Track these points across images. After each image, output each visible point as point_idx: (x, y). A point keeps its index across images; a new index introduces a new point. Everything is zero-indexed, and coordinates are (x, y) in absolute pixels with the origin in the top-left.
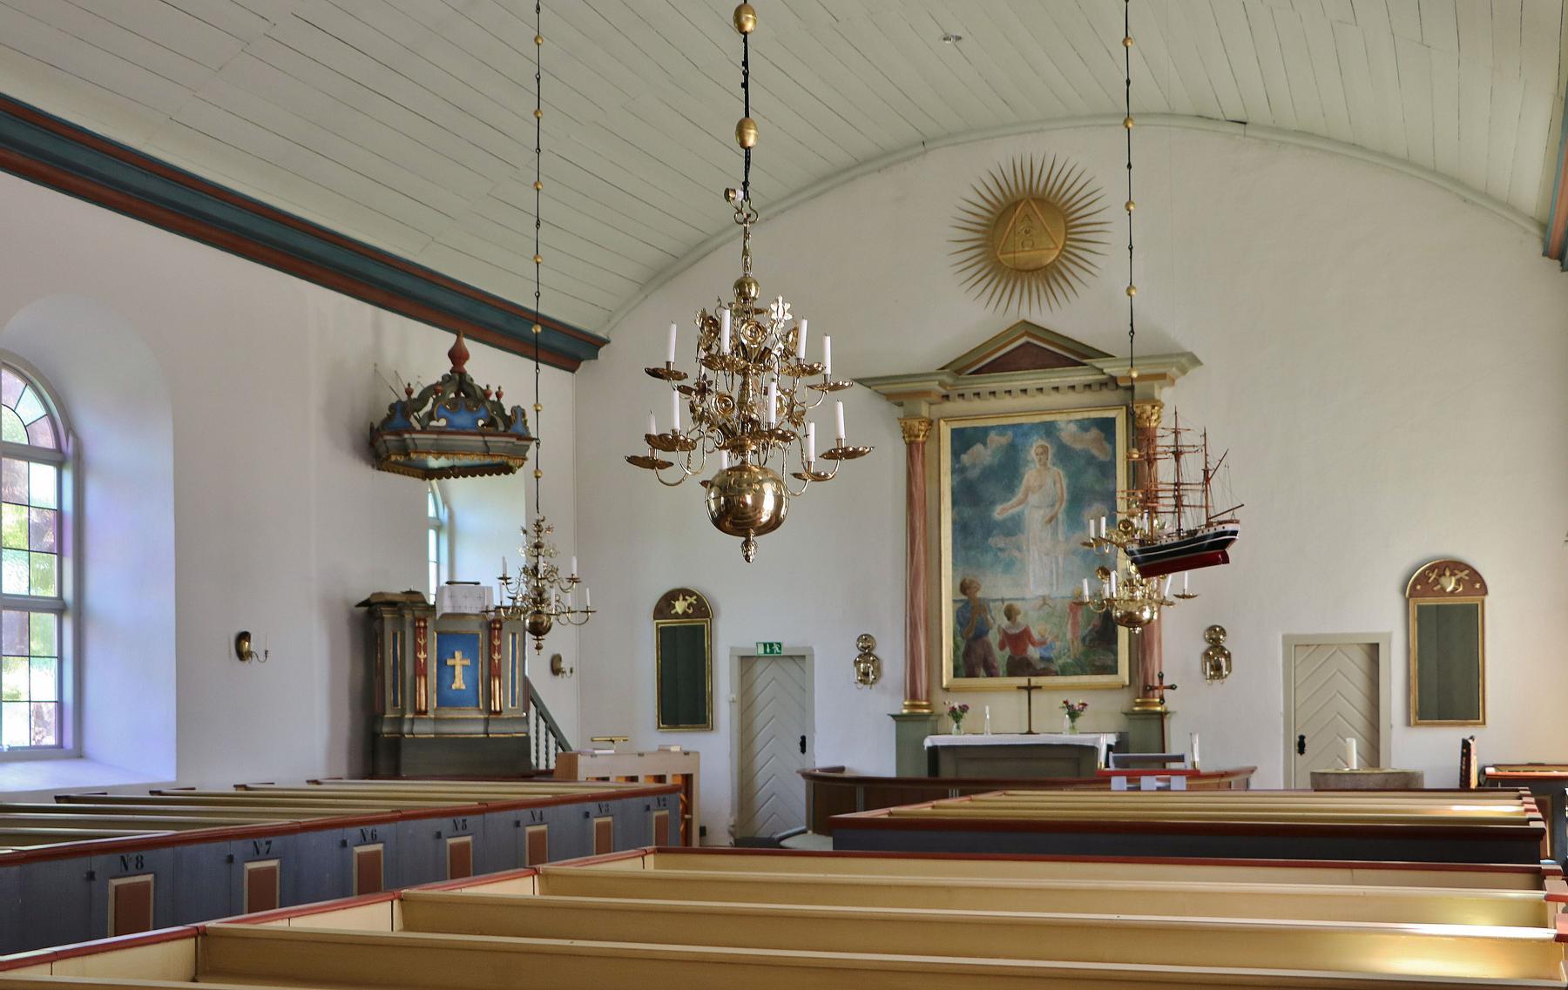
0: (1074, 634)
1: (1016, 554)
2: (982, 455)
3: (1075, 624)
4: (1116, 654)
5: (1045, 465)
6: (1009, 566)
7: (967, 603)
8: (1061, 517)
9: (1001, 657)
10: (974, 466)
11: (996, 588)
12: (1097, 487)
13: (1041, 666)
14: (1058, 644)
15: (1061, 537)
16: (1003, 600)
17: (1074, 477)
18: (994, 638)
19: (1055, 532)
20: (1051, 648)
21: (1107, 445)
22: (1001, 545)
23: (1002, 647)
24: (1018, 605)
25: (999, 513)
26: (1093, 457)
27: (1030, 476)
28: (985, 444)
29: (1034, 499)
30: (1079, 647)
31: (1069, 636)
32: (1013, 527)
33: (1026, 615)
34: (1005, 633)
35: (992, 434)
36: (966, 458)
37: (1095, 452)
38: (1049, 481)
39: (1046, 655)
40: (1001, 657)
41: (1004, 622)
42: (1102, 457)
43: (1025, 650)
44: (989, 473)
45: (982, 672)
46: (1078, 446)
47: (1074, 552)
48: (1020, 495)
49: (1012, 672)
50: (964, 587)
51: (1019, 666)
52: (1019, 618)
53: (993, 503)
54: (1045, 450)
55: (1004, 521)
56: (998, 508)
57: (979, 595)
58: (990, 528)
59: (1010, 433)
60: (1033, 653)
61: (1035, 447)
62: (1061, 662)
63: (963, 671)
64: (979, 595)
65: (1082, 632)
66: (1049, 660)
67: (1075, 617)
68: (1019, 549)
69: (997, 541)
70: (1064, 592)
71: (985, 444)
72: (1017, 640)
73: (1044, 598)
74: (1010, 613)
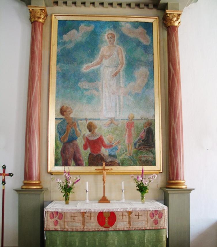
0: (129, 141)
1: (95, 92)
2: (76, 36)
3: (130, 135)
4: (154, 153)
5: (112, 44)
6: (90, 99)
7: (64, 120)
8: (122, 73)
9: (85, 154)
10: (71, 41)
11: (82, 112)
12: (143, 58)
13: (109, 160)
14: (120, 147)
15: (122, 85)
16: (86, 120)
17: (129, 52)
18: (80, 142)
19: (118, 82)
20: (115, 149)
21: (148, 37)
22: (86, 87)
23: (85, 148)
24: (96, 123)
25: (85, 68)
26: (140, 42)
27: (104, 49)
28: (78, 30)
29: (105, 62)
30: (132, 149)
31: (126, 142)
32: (93, 78)
33: (100, 129)
34: (87, 139)
35: (82, 25)
36: (66, 37)
37: (142, 40)
38: (115, 53)
39: (113, 153)
40: (85, 154)
41: (87, 133)
42: (145, 43)
43: (100, 150)
44: (79, 46)
45: (73, 162)
46: (132, 36)
47: (129, 94)
48: (97, 59)
49: (91, 164)
50: (62, 111)
51: (96, 160)
52: (96, 131)
53: (82, 63)
54: (113, 36)
55: (88, 74)
56: (85, 66)
57: (72, 116)
58: (79, 76)
59: (92, 26)
60: (104, 152)
61: (106, 34)
62: (121, 157)
63: (60, 162)
64: (72, 116)
65: (135, 140)
66: (114, 156)
67: (130, 131)
68: (97, 90)
69: (83, 84)
70: (124, 115)
71: (78, 30)
72: (95, 144)
73: (111, 119)
74: (91, 127)
